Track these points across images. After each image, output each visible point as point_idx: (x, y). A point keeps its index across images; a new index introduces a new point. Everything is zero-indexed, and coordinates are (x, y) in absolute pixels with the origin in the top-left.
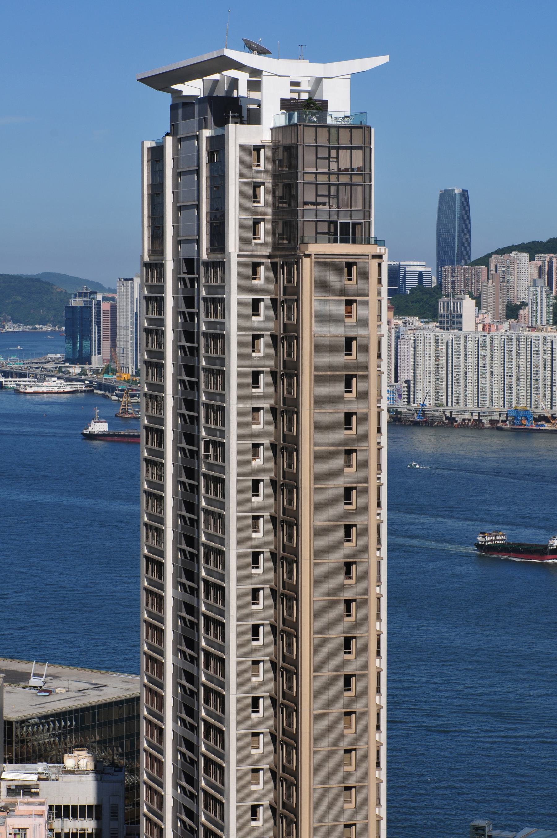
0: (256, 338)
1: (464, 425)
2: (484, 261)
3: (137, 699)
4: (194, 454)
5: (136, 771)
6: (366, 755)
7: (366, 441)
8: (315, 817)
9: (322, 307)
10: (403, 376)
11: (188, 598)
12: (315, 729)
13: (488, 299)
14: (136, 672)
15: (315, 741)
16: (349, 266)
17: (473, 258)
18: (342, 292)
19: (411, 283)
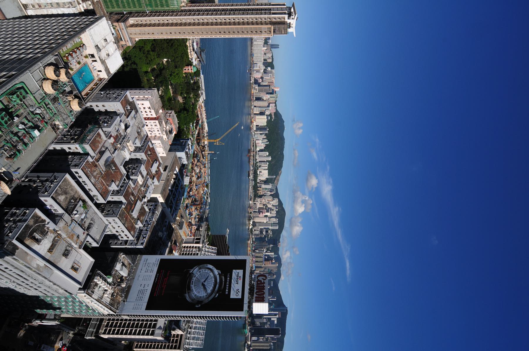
0: (261, 19)
1: (251, 48)
2: (271, 50)
3: (215, 3)
4: (246, 11)
5: (206, 3)
6: (212, 35)
7: (249, 34)
8: (203, 28)
9: (265, 28)
10: (257, 40)
11: (228, 10)
12: (214, 28)
13: (266, 51)
14: (219, 3)
15: (212, 28)
16: (270, 32)
17: (271, 49)
18: (267, 31)
19: (268, 41)
